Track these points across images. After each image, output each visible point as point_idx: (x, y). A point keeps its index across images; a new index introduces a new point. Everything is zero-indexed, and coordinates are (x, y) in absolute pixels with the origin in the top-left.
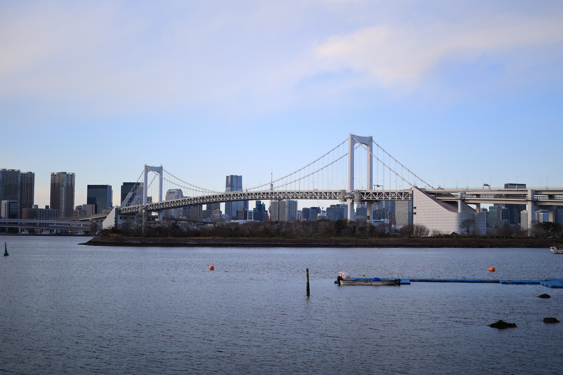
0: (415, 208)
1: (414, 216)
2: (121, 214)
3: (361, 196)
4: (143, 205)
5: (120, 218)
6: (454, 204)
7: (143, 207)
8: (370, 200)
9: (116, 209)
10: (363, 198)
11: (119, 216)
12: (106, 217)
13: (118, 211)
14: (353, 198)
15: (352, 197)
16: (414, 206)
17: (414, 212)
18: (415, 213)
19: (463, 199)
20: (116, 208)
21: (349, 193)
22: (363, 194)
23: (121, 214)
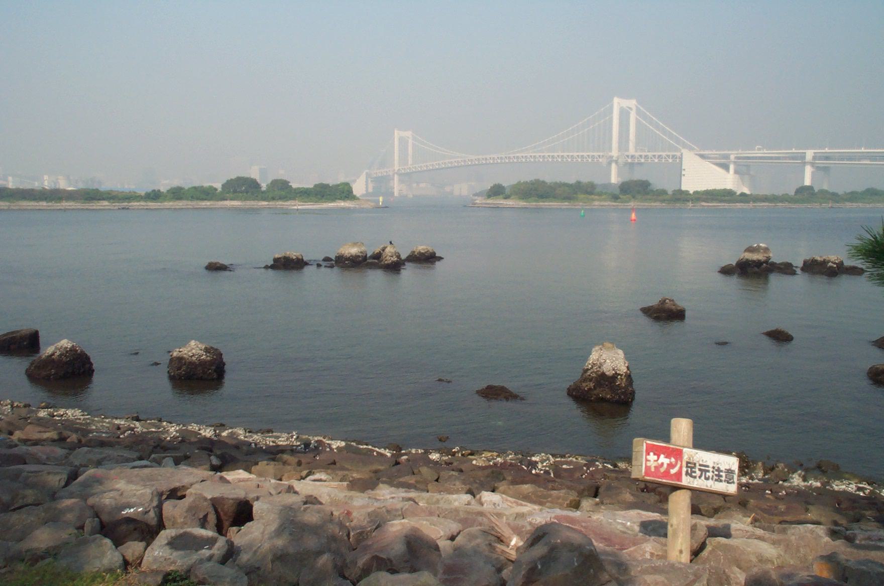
0: (684, 170)
1: (683, 178)
3: (625, 158)
6: (726, 167)
7: (396, 171)
9: (367, 173)
10: (627, 160)
11: (369, 180)
12: (356, 181)
15: (617, 159)
16: (683, 168)
18: (684, 175)
19: (736, 160)
23: (371, 178)
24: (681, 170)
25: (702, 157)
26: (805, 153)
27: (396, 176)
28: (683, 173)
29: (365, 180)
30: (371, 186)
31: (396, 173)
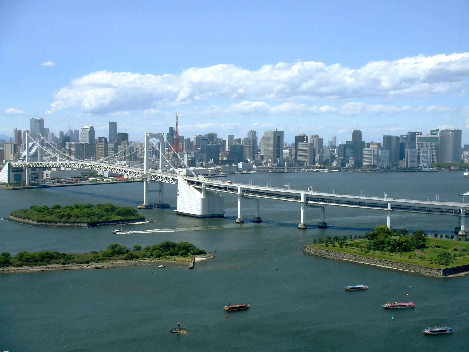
1: (178, 196)
2: (13, 168)
3: (152, 177)
4: (26, 163)
5: (11, 171)
6: (200, 190)
8: (156, 181)
9: (9, 164)
11: (11, 170)
13: (10, 166)
14: (147, 178)
15: (146, 177)
16: (178, 190)
17: (178, 194)
19: (205, 188)
20: (8, 164)
21: (145, 175)
22: (153, 176)
24: (177, 191)
25: (189, 182)
26: (238, 187)
27: (26, 168)
28: (178, 193)
29: (8, 170)
30: (12, 174)
31: (27, 167)
